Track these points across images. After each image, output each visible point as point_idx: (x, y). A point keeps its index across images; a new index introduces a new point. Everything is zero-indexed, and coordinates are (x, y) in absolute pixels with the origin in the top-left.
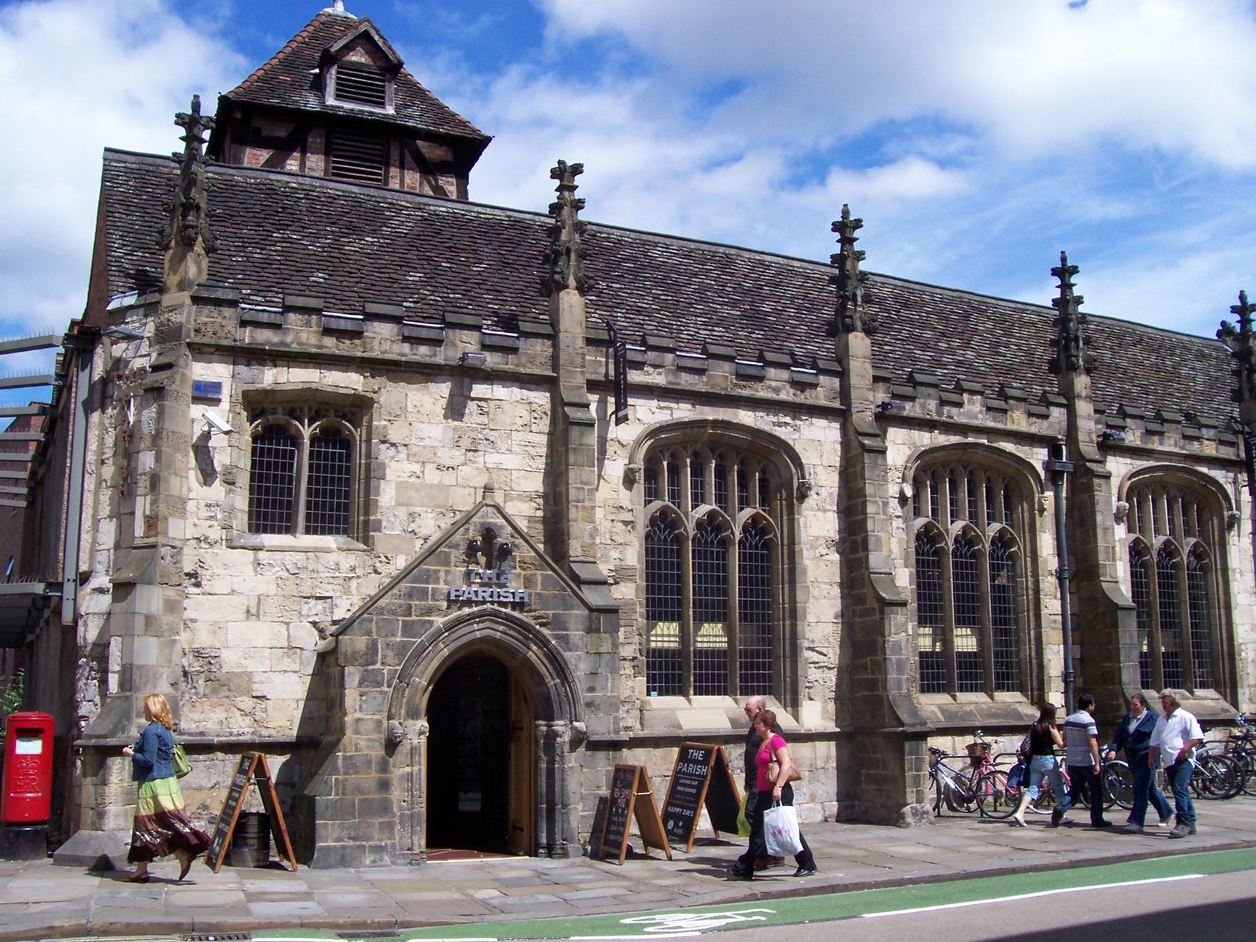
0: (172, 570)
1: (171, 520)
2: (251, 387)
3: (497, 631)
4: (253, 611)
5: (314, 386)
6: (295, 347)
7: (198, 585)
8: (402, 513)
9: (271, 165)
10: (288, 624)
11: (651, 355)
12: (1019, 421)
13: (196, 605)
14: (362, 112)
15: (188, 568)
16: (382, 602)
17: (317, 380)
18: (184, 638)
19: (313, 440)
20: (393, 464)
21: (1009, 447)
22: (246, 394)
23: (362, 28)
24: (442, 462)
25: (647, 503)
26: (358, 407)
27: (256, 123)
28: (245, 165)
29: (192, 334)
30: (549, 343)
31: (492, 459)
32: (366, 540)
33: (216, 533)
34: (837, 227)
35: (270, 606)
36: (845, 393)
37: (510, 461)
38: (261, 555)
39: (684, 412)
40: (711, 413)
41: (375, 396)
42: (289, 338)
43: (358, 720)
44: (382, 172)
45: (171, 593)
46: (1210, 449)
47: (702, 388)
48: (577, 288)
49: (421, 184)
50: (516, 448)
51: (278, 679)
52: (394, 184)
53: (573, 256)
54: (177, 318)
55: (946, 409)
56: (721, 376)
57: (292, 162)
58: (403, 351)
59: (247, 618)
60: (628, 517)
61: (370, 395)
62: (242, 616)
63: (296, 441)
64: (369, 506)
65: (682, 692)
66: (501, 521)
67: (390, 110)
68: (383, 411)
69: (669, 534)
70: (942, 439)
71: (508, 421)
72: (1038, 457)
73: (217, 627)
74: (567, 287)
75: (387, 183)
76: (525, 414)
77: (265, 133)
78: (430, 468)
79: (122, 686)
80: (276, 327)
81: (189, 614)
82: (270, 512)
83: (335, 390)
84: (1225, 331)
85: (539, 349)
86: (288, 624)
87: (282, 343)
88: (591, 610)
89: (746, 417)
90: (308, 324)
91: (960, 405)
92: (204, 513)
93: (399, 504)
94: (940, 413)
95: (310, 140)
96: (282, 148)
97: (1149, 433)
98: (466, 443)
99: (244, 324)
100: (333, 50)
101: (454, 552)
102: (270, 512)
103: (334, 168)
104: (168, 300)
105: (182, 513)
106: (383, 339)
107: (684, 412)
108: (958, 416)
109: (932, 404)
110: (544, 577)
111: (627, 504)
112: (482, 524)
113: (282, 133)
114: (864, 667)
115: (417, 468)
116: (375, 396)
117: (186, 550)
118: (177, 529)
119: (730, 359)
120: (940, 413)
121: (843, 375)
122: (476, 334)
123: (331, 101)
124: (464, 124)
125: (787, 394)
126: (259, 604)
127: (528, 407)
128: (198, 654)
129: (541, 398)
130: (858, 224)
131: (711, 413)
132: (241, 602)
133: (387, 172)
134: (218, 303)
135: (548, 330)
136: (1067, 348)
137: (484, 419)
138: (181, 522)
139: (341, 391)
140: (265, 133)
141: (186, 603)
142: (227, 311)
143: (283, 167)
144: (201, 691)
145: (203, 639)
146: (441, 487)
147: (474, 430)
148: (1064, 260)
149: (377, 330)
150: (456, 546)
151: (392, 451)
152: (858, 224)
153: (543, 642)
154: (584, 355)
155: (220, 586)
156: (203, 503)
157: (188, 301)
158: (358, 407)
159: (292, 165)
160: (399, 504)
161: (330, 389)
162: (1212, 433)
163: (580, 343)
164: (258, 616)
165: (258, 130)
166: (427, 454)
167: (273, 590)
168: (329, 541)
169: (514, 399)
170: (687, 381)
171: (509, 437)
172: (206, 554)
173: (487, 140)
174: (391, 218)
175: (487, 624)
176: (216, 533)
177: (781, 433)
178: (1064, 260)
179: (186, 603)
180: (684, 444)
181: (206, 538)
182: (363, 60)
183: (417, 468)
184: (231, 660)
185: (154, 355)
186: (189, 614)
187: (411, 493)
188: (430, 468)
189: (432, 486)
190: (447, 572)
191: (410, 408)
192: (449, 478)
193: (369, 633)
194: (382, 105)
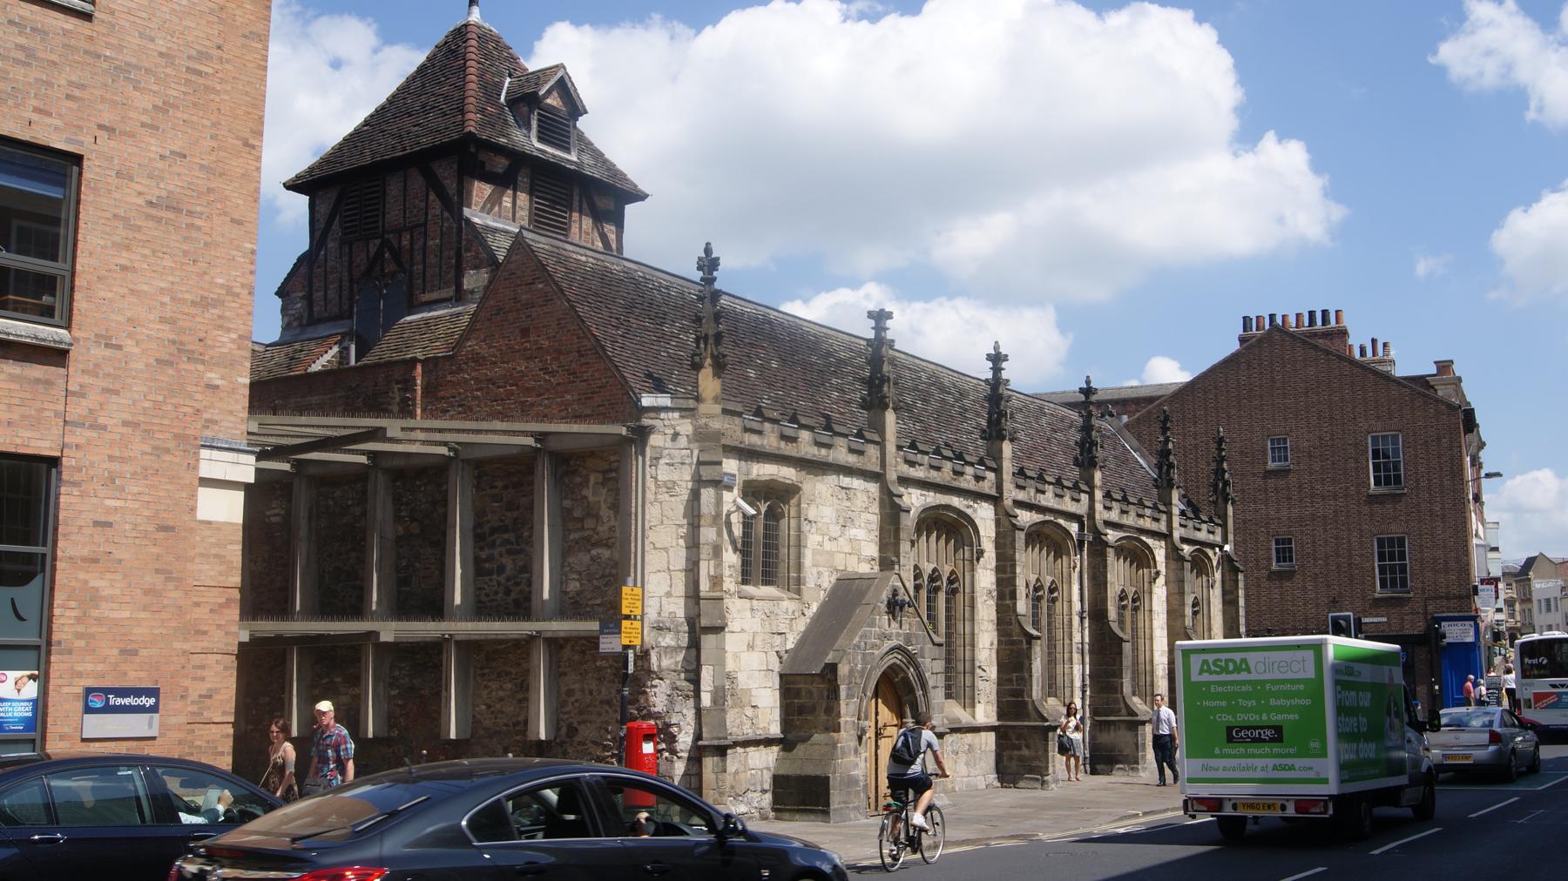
8: (815, 570)
32: (799, 592)
34: (989, 357)
35: (758, 642)
36: (999, 486)
54: (716, 425)
72: (1074, 528)
79: (714, 701)
85: (873, 451)
89: (956, 501)
97: (1123, 512)
99: (746, 430)
104: (703, 408)
106: (805, 445)
109: (1032, 491)
114: (1011, 681)
121: (998, 471)
130: (1005, 358)
132: (746, 637)
136: (1090, 451)
142: (737, 420)
146: (831, 553)
148: (1088, 382)
152: (1005, 358)
177: (969, 512)
178: (1088, 382)
184: (743, 680)
185: (696, 452)
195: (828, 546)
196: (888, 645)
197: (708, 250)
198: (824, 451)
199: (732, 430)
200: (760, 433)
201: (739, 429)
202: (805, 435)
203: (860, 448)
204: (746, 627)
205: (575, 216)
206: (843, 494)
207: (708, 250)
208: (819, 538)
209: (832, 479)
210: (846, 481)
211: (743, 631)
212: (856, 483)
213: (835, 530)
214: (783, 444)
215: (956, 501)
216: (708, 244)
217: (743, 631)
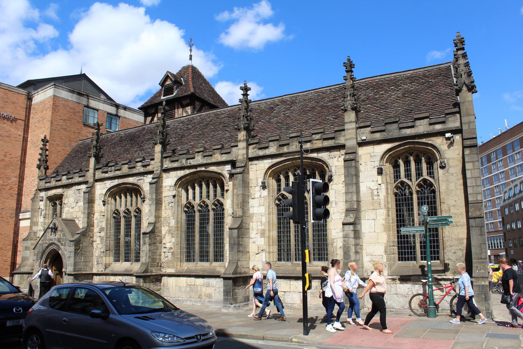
0: (34, 237)
12: (218, 157)
21: (314, 155)
22: (47, 198)
39: (116, 182)
40: (121, 181)
46: (319, 144)
47: (120, 174)
55: (189, 161)
56: (125, 169)
60: (103, 214)
69: (430, 189)
70: (187, 172)
84: (241, 101)
91: (194, 158)
94: (186, 163)
98: (76, 201)
105: (37, 225)
106: (64, 180)
107: (116, 182)
108: (193, 162)
109: (184, 161)
111: (103, 211)
120: (186, 163)
125: (142, 170)
131: (121, 181)
146: (72, 213)
162: (318, 136)
170: (118, 173)
192: (73, 210)
195: (71, 210)
198: (70, 180)
200: (49, 182)
202: (64, 178)
205: (176, 110)
208: (68, 209)
209: (75, 188)
213: (74, 205)
214: (57, 182)
215: (131, 180)
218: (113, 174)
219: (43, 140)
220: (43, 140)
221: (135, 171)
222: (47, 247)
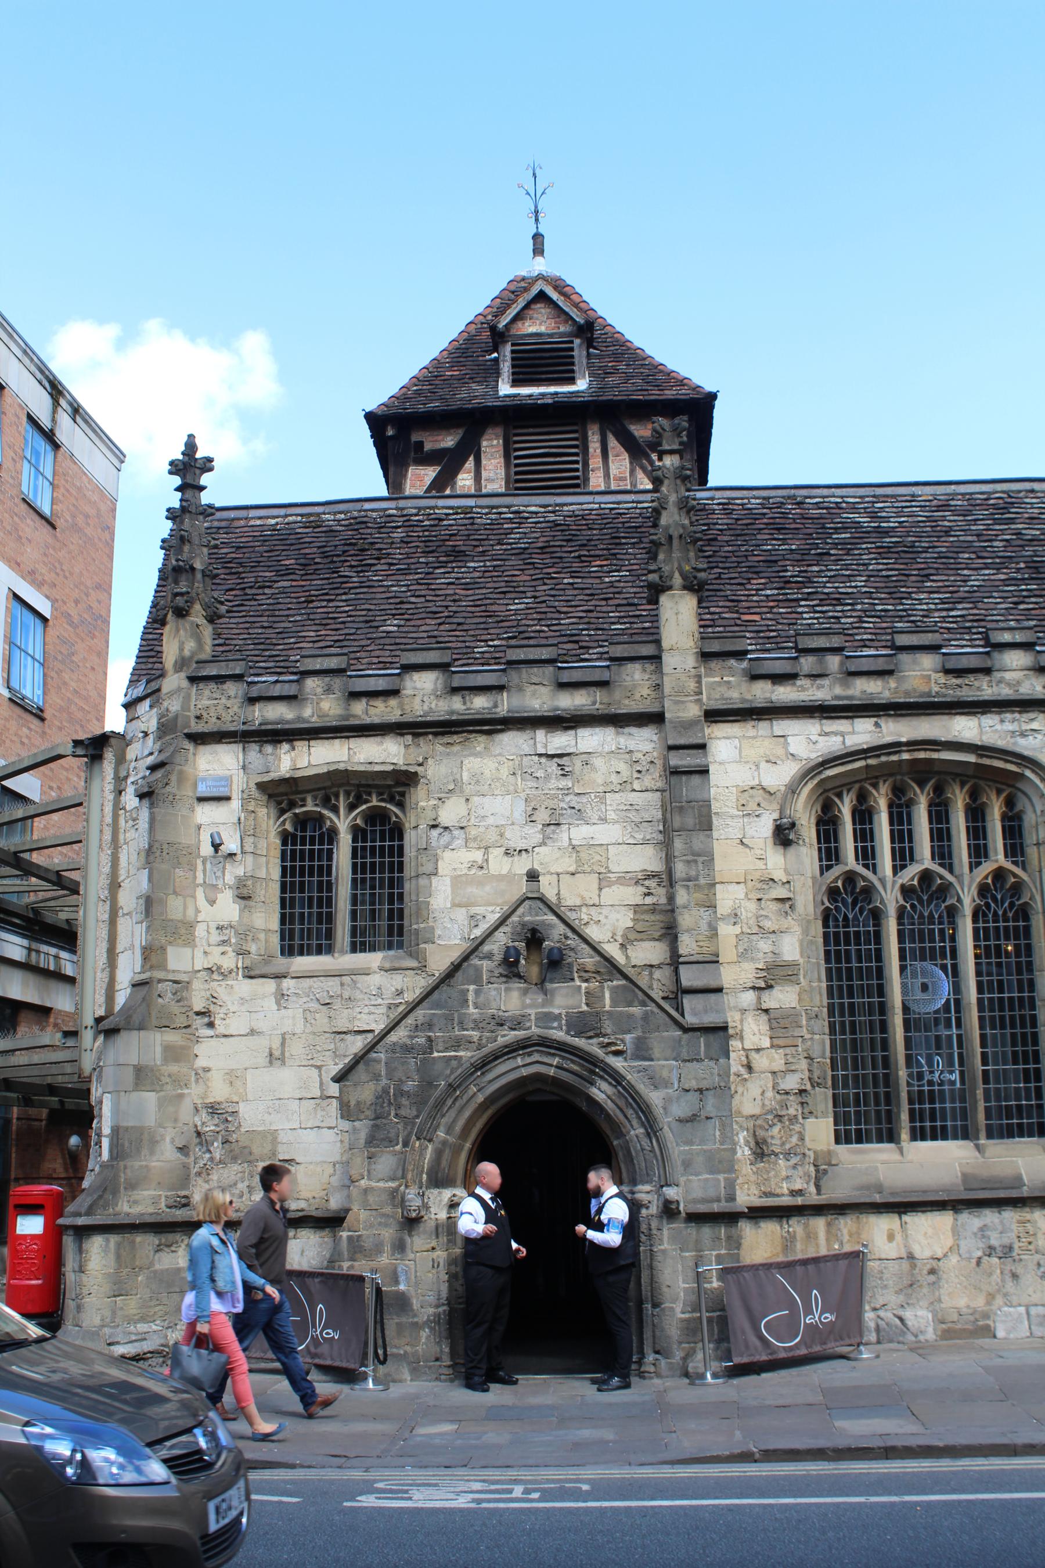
0: (176, 1009)
1: (170, 950)
2: (266, 778)
3: (550, 1065)
4: (277, 1053)
5: (342, 766)
6: (315, 721)
7: (211, 1025)
8: (461, 915)
9: (439, 485)
10: (319, 1068)
11: (807, 663)
13: (210, 1053)
14: (543, 395)
15: (198, 1005)
16: (393, 1037)
17: (345, 758)
18: (194, 1093)
19: (357, 832)
20: (447, 855)
22: (261, 786)
23: (534, 291)
24: (512, 844)
25: (823, 869)
26: (399, 783)
27: (415, 437)
28: (407, 493)
29: (193, 721)
30: (650, 667)
31: (580, 833)
33: (229, 961)
35: (296, 1049)
37: (607, 833)
38: (287, 983)
39: (862, 733)
41: (420, 769)
42: (307, 712)
43: (366, 1191)
44: (580, 466)
45: (172, 1037)
48: (684, 588)
49: (632, 472)
50: (612, 815)
51: (309, 1136)
52: (596, 481)
53: (676, 542)
56: (921, 675)
57: (465, 476)
58: (457, 706)
59: (271, 1062)
61: (412, 769)
62: (263, 1060)
63: (332, 835)
64: (422, 910)
65: (890, 1136)
66: (551, 918)
67: (582, 384)
68: (432, 787)
71: (600, 781)
73: (233, 1077)
74: (670, 588)
75: (586, 480)
76: (622, 767)
77: (428, 447)
78: (496, 853)
80: (289, 698)
81: (200, 1063)
82: (305, 926)
83: (370, 768)
85: (636, 675)
86: (319, 1068)
87: (299, 719)
88: (686, 1030)
89: (965, 728)
90: (328, 690)
92: (215, 937)
93: (455, 905)
95: (484, 443)
96: (450, 464)
98: (543, 816)
100: (501, 326)
101: (486, 964)
102: (305, 926)
103: (577, 470)
105: (190, 942)
106: (423, 693)
107: (862, 733)
110: (614, 990)
111: (779, 875)
112: (523, 925)
113: (448, 441)
115: (478, 856)
116: (420, 769)
117: (196, 985)
118: (179, 960)
119: (934, 648)
122: (549, 670)
123: (505, 389)
124: (682, 382)
126: (283, 1044)
127: (627, 756)
128: (213, 1109)
129: (643, 741)
132: (262, 1044)
133: (586, 464)
134: (220, 679)
135: (647, 650)
137: (567, 782)
138: (188, 951)
139: (377, 768)
140: (428, 447)
141: (198, 1049)
142: (232, 688)
143: (453, 488)
144: (217, 1156)
145: (219, 1091)
147: (554, 797)
149: (418, 685)
150: (489, 956)
151: (446, 837)
153: (616, 1078)
154: (700, 676)
155: (236, 1024)
156: (213, 926)
157: (185, 683)
158: (399, 783)
159: (465, 480)
160: (455, 905)
161: (362, 768)
163: (690, 661)
164: (282, 1059)
165: (420, 445)
166: (492, 836)
167: (299, 1028)
168: (374, 959)
169: (607, 749)
171: (603, 801)
172: (220, 990)
173: (712, 397)
174: (511, 531)
175: (536, 1057)
176: (229, 961)
179: (198, 1049)
180: (874, 776)
181: (219, 968)
182: (543, 329)
183: (478, 856)
186: (200, 1063)
187: (472, 890)
188: (496, 853)
189: (500, 878)
190: (477, 993)
191: (466, 776)
193: (377, 1077)
194: (572, 381)
196: (507, 1036)
197: (191, 446)
199: (222, 705)
201: (235, 705)
203: (605, 676)
204: (261, 1025)
206: (552, 766)
207: (191, 446)
209: (513, 742)
210: (559, 741)
211: (253, 1032)
212: (590, 740)
216: (191, 437)
217: (253, 1032)
218: (838, 691)
219: (176, 468)
220: (176, 468)
221: (986, 689)
222: (484, 1064)
